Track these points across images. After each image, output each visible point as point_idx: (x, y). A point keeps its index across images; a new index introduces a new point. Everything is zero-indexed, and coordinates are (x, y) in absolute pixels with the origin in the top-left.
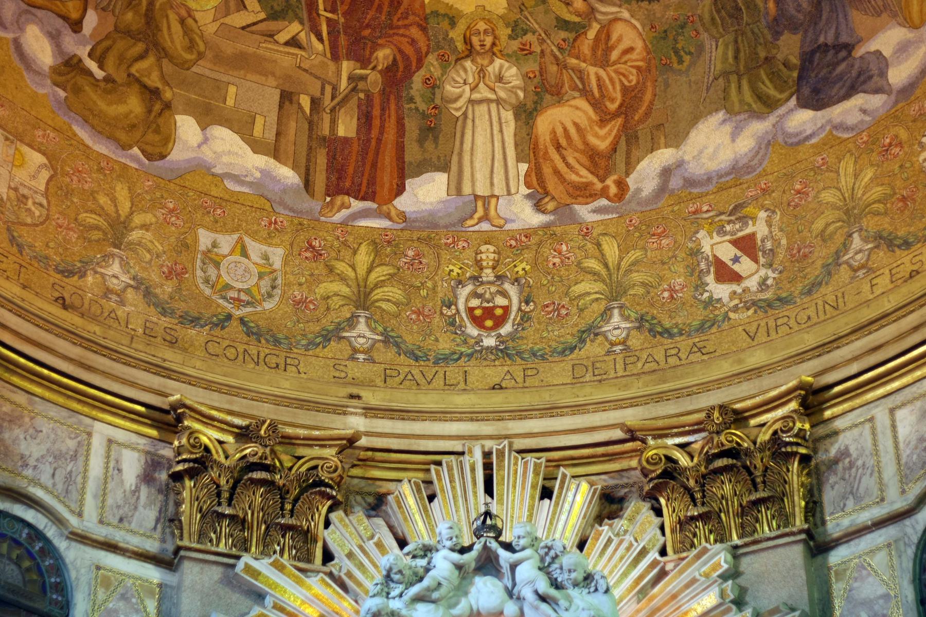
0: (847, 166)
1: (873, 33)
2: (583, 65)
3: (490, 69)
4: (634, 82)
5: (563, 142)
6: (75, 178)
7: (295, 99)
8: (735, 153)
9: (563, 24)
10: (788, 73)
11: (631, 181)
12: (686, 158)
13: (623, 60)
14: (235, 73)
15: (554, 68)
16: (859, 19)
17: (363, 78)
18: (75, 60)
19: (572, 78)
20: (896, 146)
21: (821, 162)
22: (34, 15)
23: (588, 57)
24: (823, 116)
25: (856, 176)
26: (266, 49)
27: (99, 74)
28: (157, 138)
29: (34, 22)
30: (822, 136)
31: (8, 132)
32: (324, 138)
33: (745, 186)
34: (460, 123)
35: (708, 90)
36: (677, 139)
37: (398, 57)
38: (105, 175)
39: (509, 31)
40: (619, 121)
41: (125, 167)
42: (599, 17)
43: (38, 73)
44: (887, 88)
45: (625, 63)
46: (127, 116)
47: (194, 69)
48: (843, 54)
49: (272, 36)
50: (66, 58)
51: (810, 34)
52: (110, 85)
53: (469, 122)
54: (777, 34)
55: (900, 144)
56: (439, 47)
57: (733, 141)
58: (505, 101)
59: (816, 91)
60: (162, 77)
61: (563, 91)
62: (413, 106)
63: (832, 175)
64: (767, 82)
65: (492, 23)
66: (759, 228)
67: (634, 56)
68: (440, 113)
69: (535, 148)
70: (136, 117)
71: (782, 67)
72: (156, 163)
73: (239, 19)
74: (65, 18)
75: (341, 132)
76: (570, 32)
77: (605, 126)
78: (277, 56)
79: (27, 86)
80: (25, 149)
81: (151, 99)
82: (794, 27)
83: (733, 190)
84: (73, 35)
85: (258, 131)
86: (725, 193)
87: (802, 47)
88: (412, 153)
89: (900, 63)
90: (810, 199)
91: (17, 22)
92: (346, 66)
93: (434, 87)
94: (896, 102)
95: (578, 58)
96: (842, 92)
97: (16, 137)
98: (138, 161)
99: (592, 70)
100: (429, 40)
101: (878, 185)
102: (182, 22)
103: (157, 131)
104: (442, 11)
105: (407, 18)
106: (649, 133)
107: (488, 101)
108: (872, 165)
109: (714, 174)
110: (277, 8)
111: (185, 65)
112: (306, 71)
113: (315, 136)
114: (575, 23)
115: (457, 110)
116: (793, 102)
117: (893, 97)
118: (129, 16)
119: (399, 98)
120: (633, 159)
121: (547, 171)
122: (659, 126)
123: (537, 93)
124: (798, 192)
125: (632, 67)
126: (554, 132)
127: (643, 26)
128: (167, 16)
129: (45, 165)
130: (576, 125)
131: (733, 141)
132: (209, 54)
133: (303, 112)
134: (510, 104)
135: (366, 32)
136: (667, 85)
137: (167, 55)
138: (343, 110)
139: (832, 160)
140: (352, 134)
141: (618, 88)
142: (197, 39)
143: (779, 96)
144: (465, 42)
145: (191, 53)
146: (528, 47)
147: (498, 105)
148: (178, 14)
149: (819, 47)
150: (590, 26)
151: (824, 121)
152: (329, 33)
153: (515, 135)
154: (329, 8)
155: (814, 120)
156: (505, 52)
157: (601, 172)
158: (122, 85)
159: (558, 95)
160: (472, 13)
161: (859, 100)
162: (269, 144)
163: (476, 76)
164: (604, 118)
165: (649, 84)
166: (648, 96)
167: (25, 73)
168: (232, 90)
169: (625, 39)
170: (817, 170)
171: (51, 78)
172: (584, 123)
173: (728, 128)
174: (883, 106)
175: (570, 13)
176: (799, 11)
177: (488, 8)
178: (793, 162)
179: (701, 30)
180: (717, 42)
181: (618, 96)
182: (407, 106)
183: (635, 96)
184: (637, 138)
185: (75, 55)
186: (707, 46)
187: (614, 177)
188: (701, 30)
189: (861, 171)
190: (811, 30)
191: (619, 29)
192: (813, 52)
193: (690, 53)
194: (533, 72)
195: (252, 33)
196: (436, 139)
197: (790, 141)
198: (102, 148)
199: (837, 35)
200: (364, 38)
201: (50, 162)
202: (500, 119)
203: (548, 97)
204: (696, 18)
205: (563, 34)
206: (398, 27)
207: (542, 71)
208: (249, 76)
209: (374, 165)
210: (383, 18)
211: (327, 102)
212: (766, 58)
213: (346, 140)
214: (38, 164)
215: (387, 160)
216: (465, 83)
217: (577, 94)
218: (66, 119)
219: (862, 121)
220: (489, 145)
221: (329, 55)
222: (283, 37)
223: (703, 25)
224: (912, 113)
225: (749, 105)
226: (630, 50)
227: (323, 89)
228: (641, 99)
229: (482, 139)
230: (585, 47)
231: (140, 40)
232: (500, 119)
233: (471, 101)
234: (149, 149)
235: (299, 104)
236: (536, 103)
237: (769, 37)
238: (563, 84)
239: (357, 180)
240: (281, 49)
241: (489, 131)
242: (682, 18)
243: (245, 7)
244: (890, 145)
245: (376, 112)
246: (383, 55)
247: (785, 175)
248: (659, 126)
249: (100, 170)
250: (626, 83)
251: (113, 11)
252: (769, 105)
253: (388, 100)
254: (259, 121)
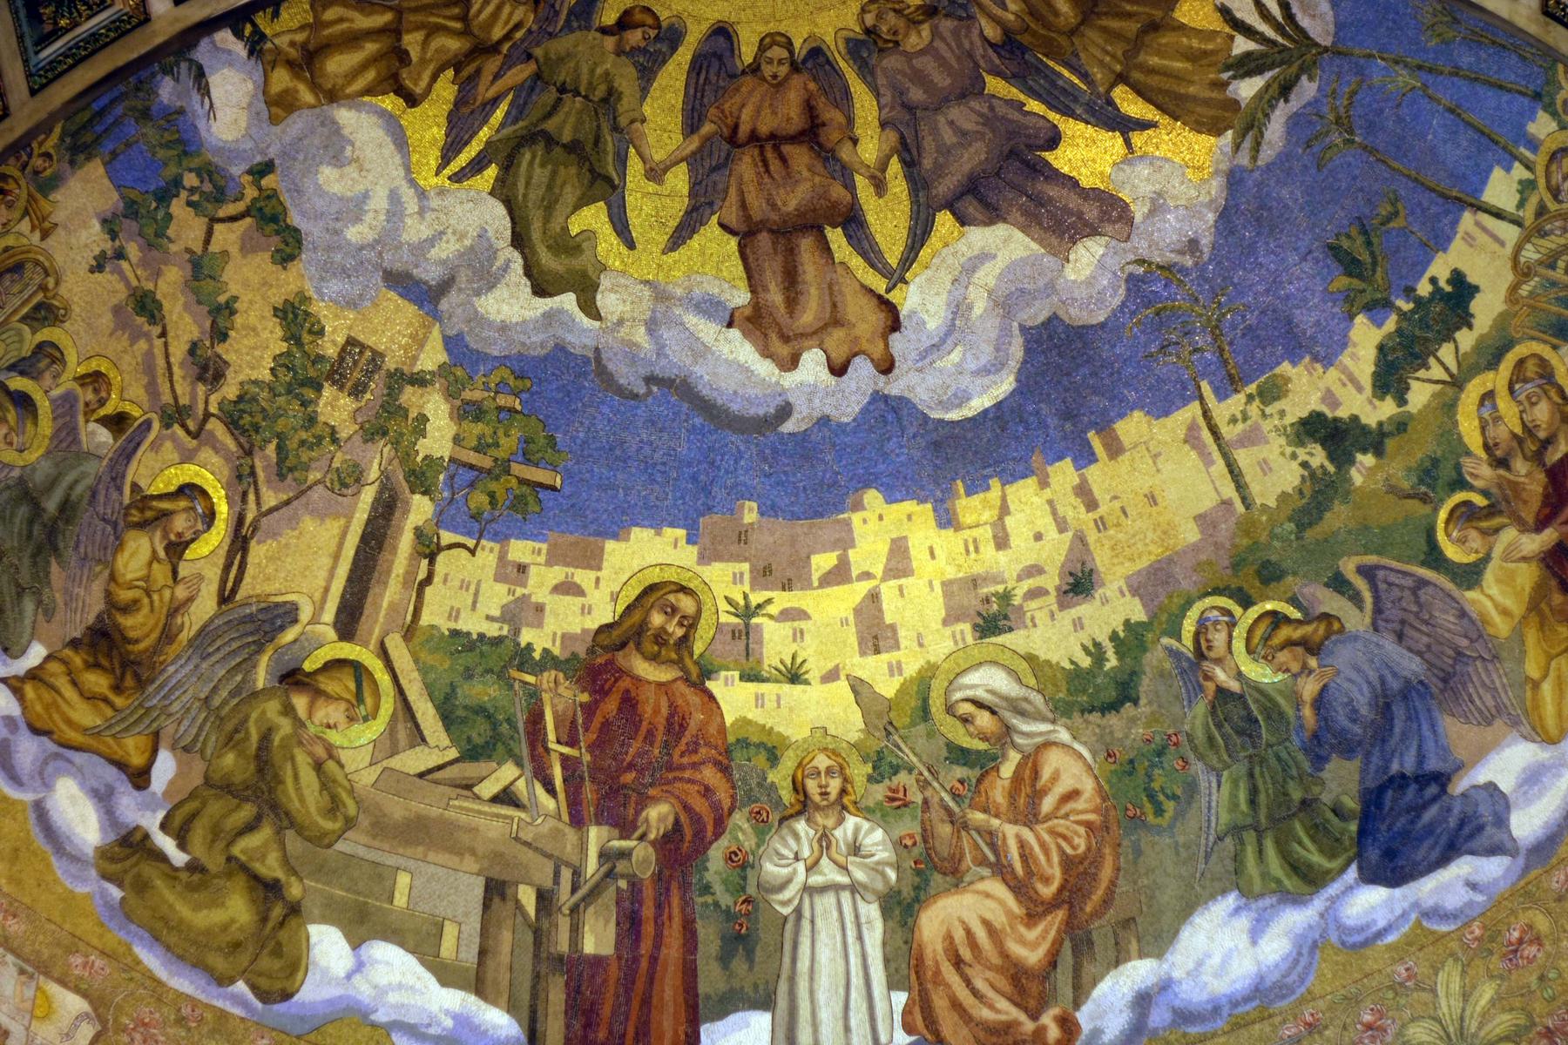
0: (1449, 980)
1: (1482, 753)
2: (995, 822)
3: (838, 833)
4: (1082, 848)
5: (966, 954)
6: (138, 1037)
7: (509, 892)
8: (1258, 963)
9: (960, 755)
10: (1342, 825)
11: (1084, 1017)
12: (1177, 974)
13: (1062, 812)
14: (409, 852)
15: (945, 830)
16: (1455, 731)
17: (625, 854)
18: (138, 836)
19: (977, 846)
20: (1531, 942)
21: (1404, 974)
22: (69, 761)
23: (1003, 809)
24: (1405, 897)
25: (1466, 996)
26: (461, 810)
27: (179, 858)
28: (277, 964)
29: (69, 774)
30: (1405, 929)
31: (27, 961)
32: (560, 958)
33: (1277, 1020)
34: (789, 926)
35: (1207, 856)
36: (1159, 942)
37: (683, 818)
38: (189, 1030)
39: (869, 769)
40: (1060, 915)
41: (223, 1015)
42: (1019, 740)
43: (76, 859)
44: (1509, 845)
45: (1066, 816)
46: (225, 928)
47: (340, 846)
48: (1433, 790)
49: (469, 787)
50: (123, 832)
51: (1376, 759)
52: (196, 877)
53: (806, 924)
54: (1319, 761)
55: (1538, 940)
56: (750, 798)
57: (1254, 942)
58: (865, 887)
59: (1390, 854)
60: (285, 861)
61: (963, 867)
62: (709, 899)
63: (1425, 996)
64: (1306, 841)
65: (839, 755)
67: (1080, 804)
68: (756, 909)
69: (918, 965)
70: (241, 929)
71: (1330, 815)
72: (276, 1007)
73: (414, 761)
74: (121, 765)
75: (589, 946)
76: (972, 767)
77: (1035, 924)
78: (481, 822)
79: (56, 881)
80: (53, 988)
81: (266, 898)
82: (1347, 749)
83: (1257, 1027)
84: (136, 793)
85: (448, 948)
86: (1244, 1033)
87: (1362, 781)
88: (710, 979)
89: (1529, 802)
90: (1389, 1039)
91: (41, 773)
92: (596, 836)
93: (744, 866)
94: (1526, 869)
95: (985, 810)
96: (1435, 855)
97: (37, 968)
98: (244, 1004)
99: (1011, 831)
100: (733, 787)
101: (1504, 1010)
102: (318, 766)
103: (277, 952)
104: (755, 739)
105: (696, 751)
106: (1110, 934)
107: (836, 888)
108: (1492, 977)
109: (1224, 1001)
110: (478, 740)
111: (322, 840)
112: (527, 844)
113: (544, 955)
114: (978, 752)
115: (785, 903)
116: (1352, 873)
117: (1521, 861)
118: (229, 759)
119: (685, 887)
120: (1086, 978)
121: (940, 1003)
122: (1128, 922)
123: (918, 873)
124: (1369, 1027)
125: (1078, 823)
126: (949, 938)
127: (1094, 754)
128: (293, 759)
129: (87, 1014)
130: (987, 924)
131: (1254, 942)
132: (364, 821)
133: (525, 915)
134: (874, 892)
135: (629, 777)
136: (1138, 852)
137: (292, 824)
138: (591, 910)
139: (1422, 970)
140: (608, 949)
141: (1056, 859)
142: (344, 795)
143: (1328, 865)
144: (795, 789)
145: (335, 819)
146: (901, 795)
147: (853, 893)
148: (310, 754)
149: (1391, 780)
150: (1004, 756)
151: (1406, 905)
152: (565, 780)
153: (884, 944)
154: (565, 738)
155: (1388, 903)
156: (862, 805)
157: (1032, 1003)
158: (216, 876)
159: (955, 875)
160: (805, 740)
161: (1462, 867)
162: (467, 969)
163: (816, 846)
164: (1035, 911)
165: (1107, 851)
166: (1106, 873)
167: (53, 860)
168: (403, 880)
169: (1064, 776)
170: (1397, 988)
171: (97, 867)
172: (999, 920)
173: (1244, 922)
174: (1504, 877)
175: (971, 735)
176: (1354, 721)
177: (832, 731)
178: (1357, 976)
179: (1191, 756)
180: (1219, 776)
181: (1056, 873)
182: (700, 900)
183: (1085, 873)
184: (1090, 943)
185: (137, 828)
186: (1203, 785)
187: (1054, 1011)
188: (1191, 756)
189: (1474, 987)
190: (1376, 751)
191: (1053, 761)
192: (1382, 789)
193: (1174, 797)
194: (911, 836)
195: (436, 782)
196: (750, 956)
197: (1351, 940)
198: (183, 983)
199: (1421, 759)
200: (625, 786)
201: (95, 1010)
202: (857, 917)
203: (937, 878)
204: (1182, 738)
205: (960, 772)
206: (682, 768)
207: (927, 835)
208: (431, 856)
209: (646, 1002)
210: (656, 751)
211: (565, 896)
212: (1304, 802)
213: (597, 962)
214: (75, 1014)
215: (668, 993)
216: (797, 858)
217: (986, 872)
218: (122, 935)
219: (1470, 904)
220: (841, 962)
221: (566, 817)
222: (488, 789)
223: (1195, 749)
224: (1555, 886)
225: (1278, 881)
226: (1073, 795)
227: (557, 874)
228: (1095, 877)
229: (827, 954)
230: (998, 791)
231: (247, 800)
232: (857, 917)
233: (807, 889)
234: (264, 983)
235: (517, 901)
236: (917, 888)
237: (1306, 766)
238: (962, 855)
239: (618, 1028)
240: (486, 809)
241: (839, 938)
242: (1157, 738)
243: (424, 740)
244: (1520, 941)
245: (648, 911)
246: (658, 815)
247: (1345, 998)
248: (1128, 922)
249: (181, 1021)
250: (1069, 851)
251: (202, 751)
252: (1311, 880)
253: (668, 890)
254: (450, 931)
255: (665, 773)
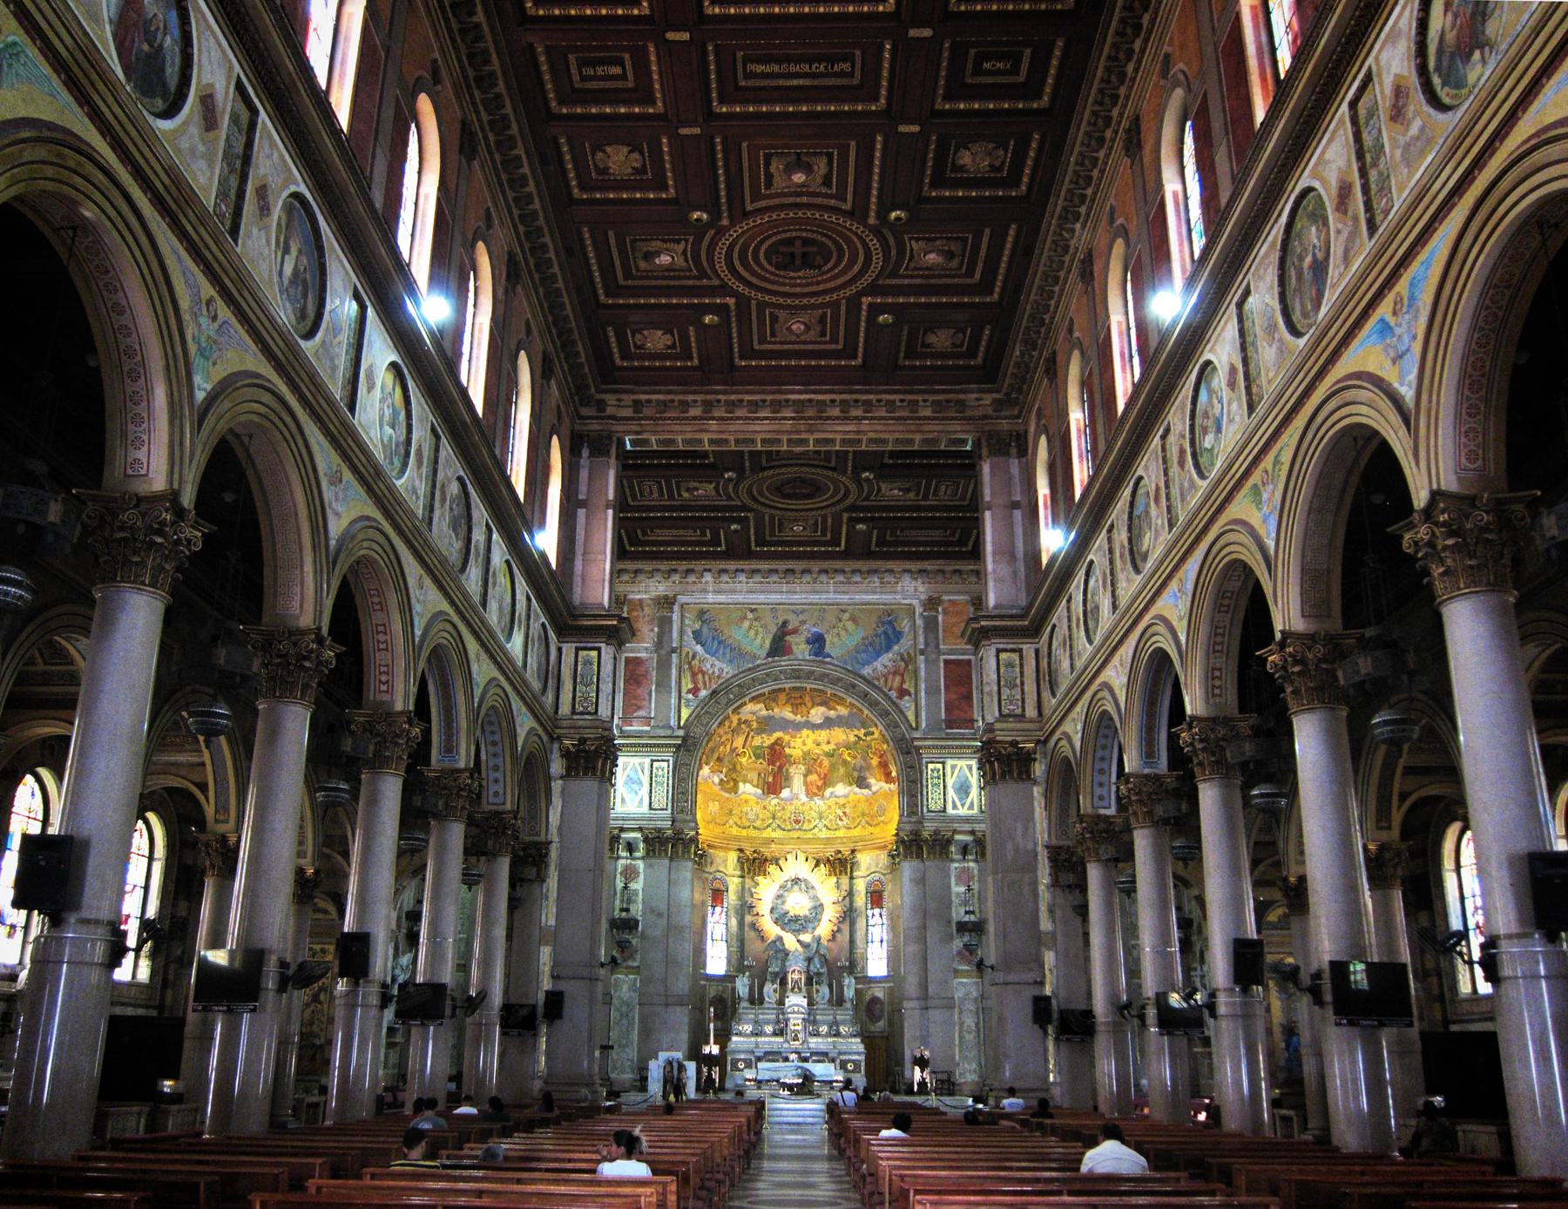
66: (847, 810)
198: (727, 795)
252: (851, 785)
255: (779, 759)
